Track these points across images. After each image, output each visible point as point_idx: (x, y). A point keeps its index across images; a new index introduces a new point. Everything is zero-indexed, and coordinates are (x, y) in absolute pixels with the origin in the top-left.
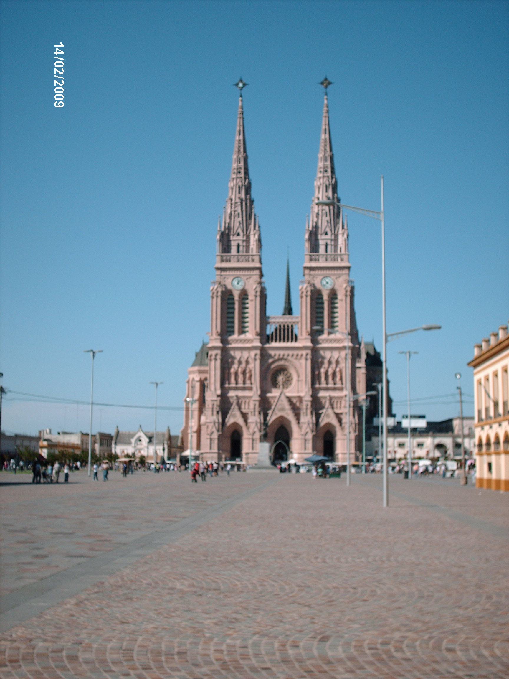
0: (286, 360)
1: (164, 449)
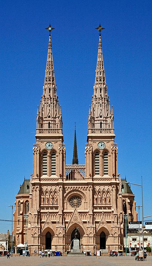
1: (6, 244)
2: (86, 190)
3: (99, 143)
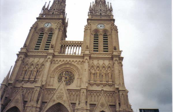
0: (71, 64)
2: (81, 64)
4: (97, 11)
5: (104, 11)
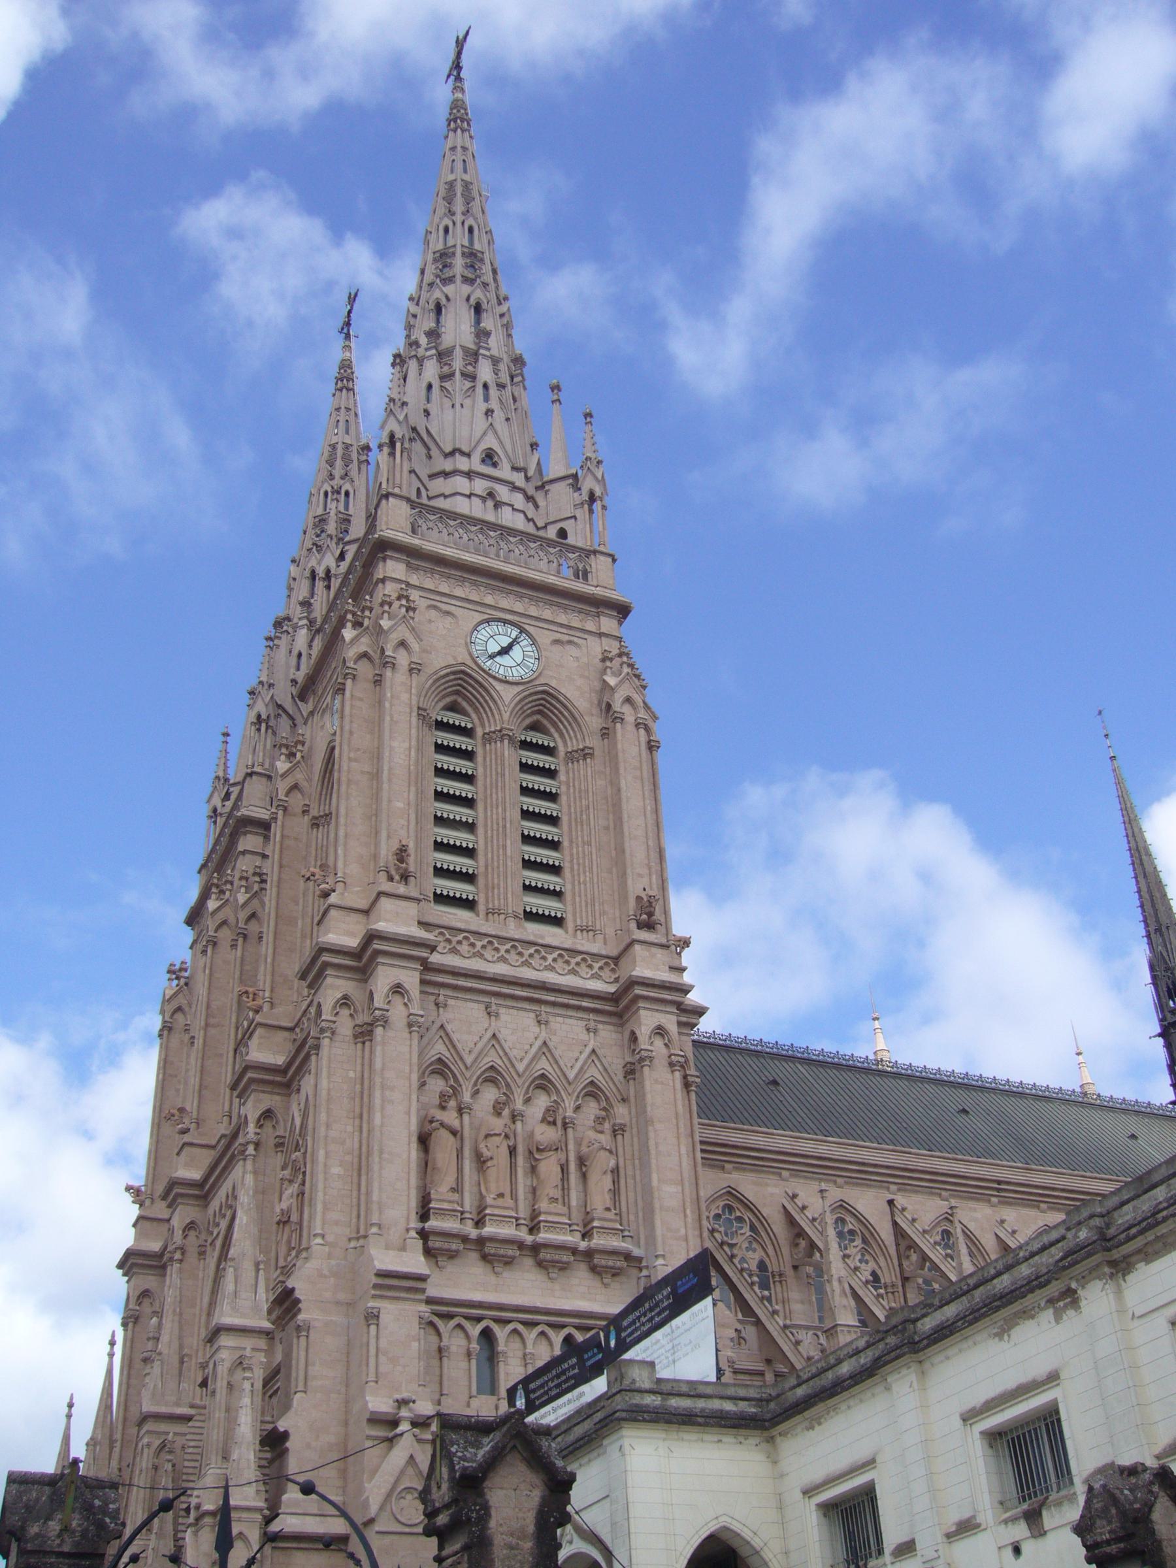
3: (488, 621)
4: (462, 464)
5: (518, 479)
